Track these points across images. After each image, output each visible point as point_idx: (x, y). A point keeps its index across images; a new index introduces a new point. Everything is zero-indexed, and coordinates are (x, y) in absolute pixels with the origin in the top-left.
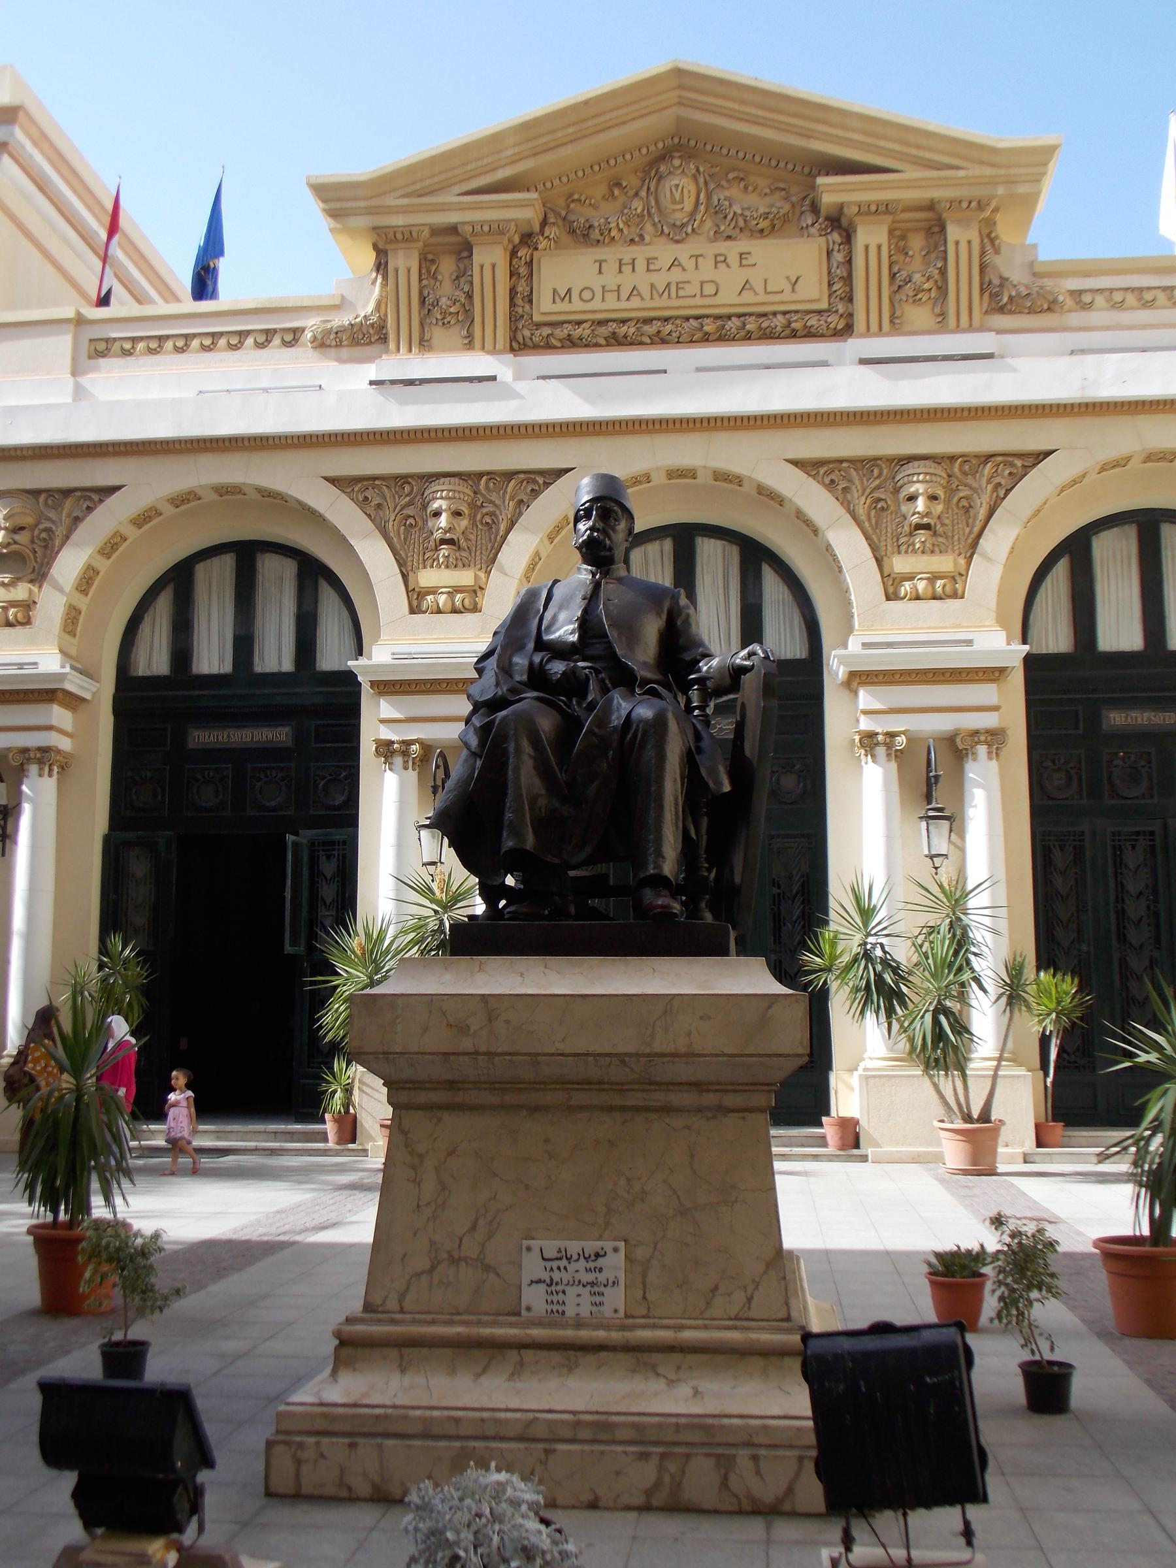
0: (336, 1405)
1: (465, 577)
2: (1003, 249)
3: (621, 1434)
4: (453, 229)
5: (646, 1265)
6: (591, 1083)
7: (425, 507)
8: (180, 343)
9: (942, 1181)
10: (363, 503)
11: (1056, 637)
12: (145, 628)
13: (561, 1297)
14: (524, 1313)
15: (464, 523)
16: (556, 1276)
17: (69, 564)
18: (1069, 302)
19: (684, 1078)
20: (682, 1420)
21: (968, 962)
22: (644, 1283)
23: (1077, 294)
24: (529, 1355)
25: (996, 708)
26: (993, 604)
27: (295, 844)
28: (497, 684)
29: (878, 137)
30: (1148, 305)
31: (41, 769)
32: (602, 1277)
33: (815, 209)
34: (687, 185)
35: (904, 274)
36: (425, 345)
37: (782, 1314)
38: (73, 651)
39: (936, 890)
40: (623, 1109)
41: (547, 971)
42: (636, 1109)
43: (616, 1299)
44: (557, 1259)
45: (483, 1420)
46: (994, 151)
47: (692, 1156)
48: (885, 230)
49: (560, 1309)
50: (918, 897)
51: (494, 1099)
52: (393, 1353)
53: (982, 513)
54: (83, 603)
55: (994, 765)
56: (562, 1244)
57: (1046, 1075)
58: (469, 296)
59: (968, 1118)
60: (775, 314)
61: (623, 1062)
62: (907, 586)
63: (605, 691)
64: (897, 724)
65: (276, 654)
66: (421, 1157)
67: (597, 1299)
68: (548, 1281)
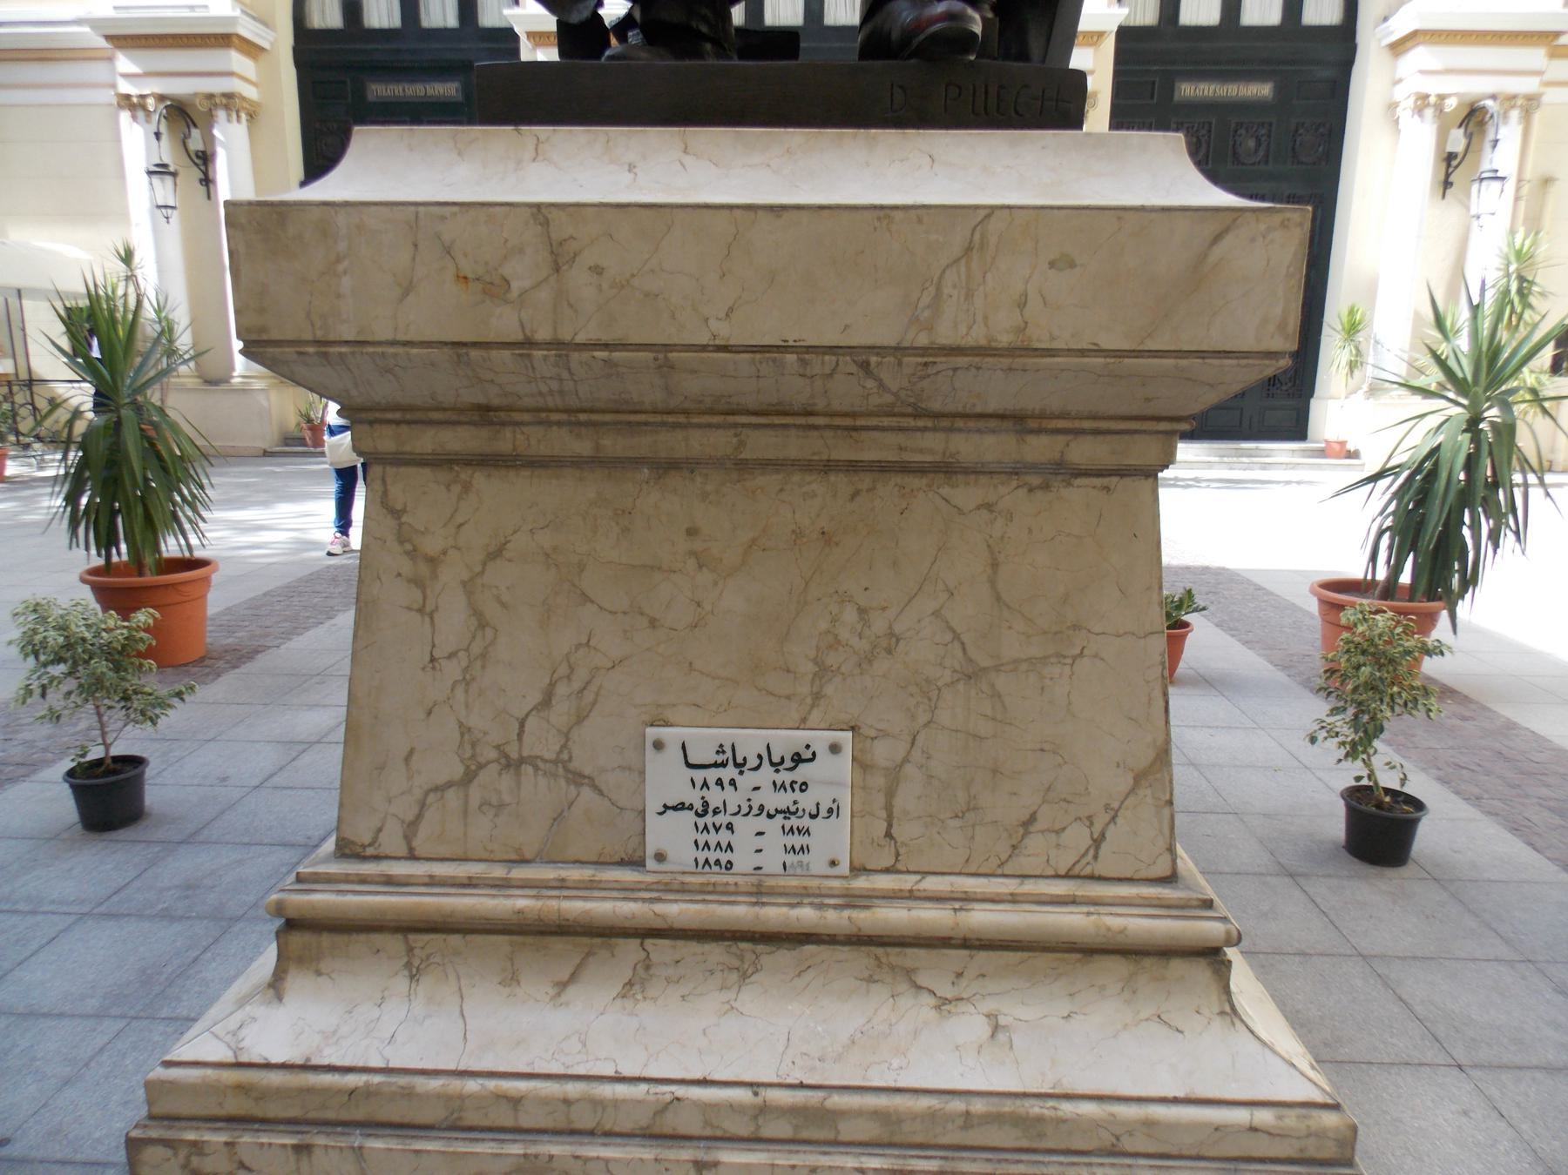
0: (268, 1066)
3: (848, 1131)
5: (894, 775)
6: (786, 414)
13: (724, 837)
14: (651, 864)
16: (715, 797)
19: (993, 406)
20: (978, 1106)
22: (889, 808)
24: (660, 949)
31: (229, 116)
32: (806, 801)
37: (1162, 869)
40: (853, 467)
41: (688, 160)
43: (832, 841)
44: (716, 765)
45: (567, 1102)
47: (995, 565)
49: (724, 857)
51: (582, 446)
52: (394, 943)
56: (726, 735)
61: (865, 366)
66: (433, 561)
68: (698, 806)
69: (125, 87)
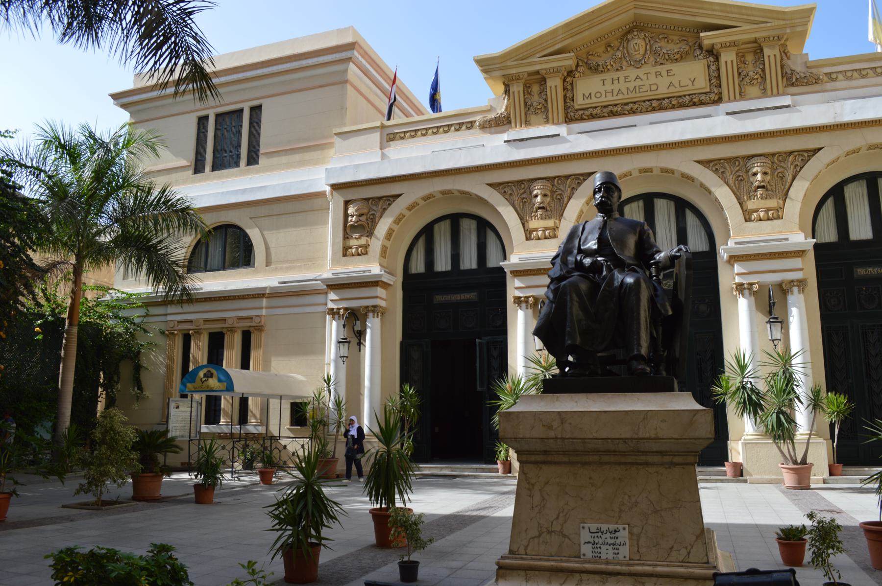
1: (550, 223)
2: (792, 57)
4: (537, 72)
7: (531, 193)
8: (424, 132)
9: (784, 492)
10: (504, 194)
11: (829, 234)
12: (414, 253)
13: (599, 550)
15: (548, 199)
16: (597, 540)
17: (383, 226)
18: (825, 78)
19: (655, 450)
21: (793, 389)
23: (829, 75)
24: (584, 576)
25: (801, 270)
26: (797, 220)
27: (480, 343)
28: (561, 270)
29: (728, 12)
30: (864, 77)
32: (618, 541)
33: (701, 47)
34: (641, 43)
35: (745, 72)
36: (527, 123)
37: (705, 560)
38: (385, 265)
39: (776, 356)
40: (625, 464)
42: (632, 464)
43: (624, 552)
46: (784, 13)
48: (734, 53)
50: (767, 359)
51: (566, 459)
52: (523, 573)
53: (790, 178)
54: (388, 244)
55: (802, 296)
56: (599, 526)
57: (833, 442)
58: (546, 100)
59: (795, 462)
60: (685, 96)
62: (755, 215)
63: (610, 270)
64: (754, 279)
65: (469, 261)
66: (533, 485)
67: (616, 551)
69: (331, 305)
